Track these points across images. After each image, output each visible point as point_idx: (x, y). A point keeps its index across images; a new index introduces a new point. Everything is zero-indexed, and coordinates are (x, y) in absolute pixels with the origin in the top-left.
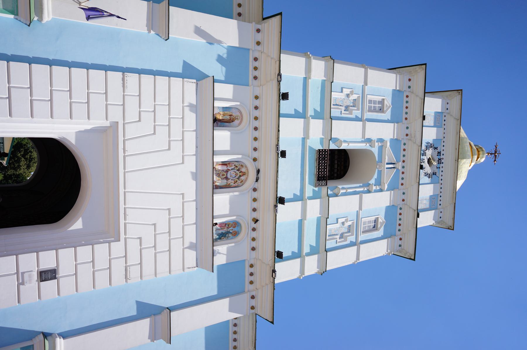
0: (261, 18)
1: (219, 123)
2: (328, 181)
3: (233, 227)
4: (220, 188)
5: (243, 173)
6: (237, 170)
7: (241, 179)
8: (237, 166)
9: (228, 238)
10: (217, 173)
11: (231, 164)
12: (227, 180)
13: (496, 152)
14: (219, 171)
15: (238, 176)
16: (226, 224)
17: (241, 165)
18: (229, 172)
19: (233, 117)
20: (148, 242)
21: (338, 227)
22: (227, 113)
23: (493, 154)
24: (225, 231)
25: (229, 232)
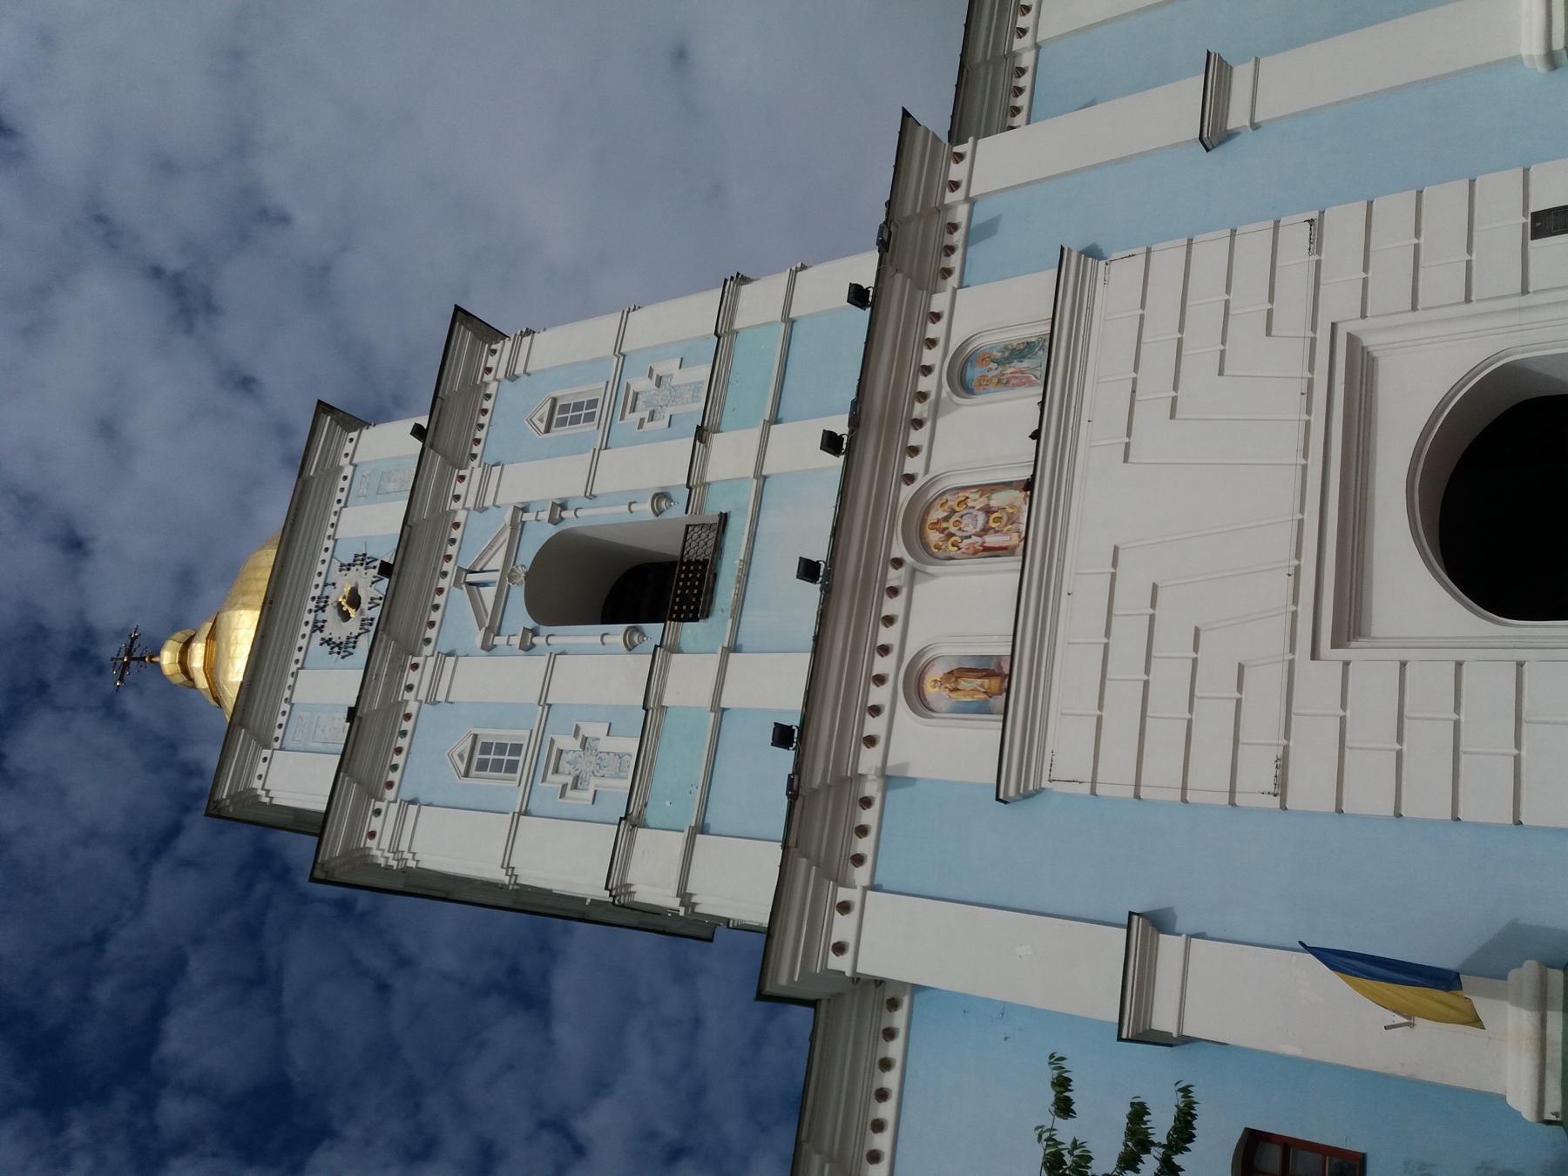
0: (823, 1008)
1: (992, 668)
3: (987, 376)
4: (1012, 482)
5: (938, 527)
6: (952, 535)
7: (944, 511)
8: (953, 545)
9: (1006, 348)
10: (1014, 526)
11: (971, 550)
12: (988, 505)
13: (126, 665)
14: (1008, 530)
15: (954, 519)
17: (939, 550)
18: (978, 530)
19: (948, 686)
21: (671, 406)
22: (965, 696)
23: (135, 659)
24: (1013, 365)
25: (998, 363)
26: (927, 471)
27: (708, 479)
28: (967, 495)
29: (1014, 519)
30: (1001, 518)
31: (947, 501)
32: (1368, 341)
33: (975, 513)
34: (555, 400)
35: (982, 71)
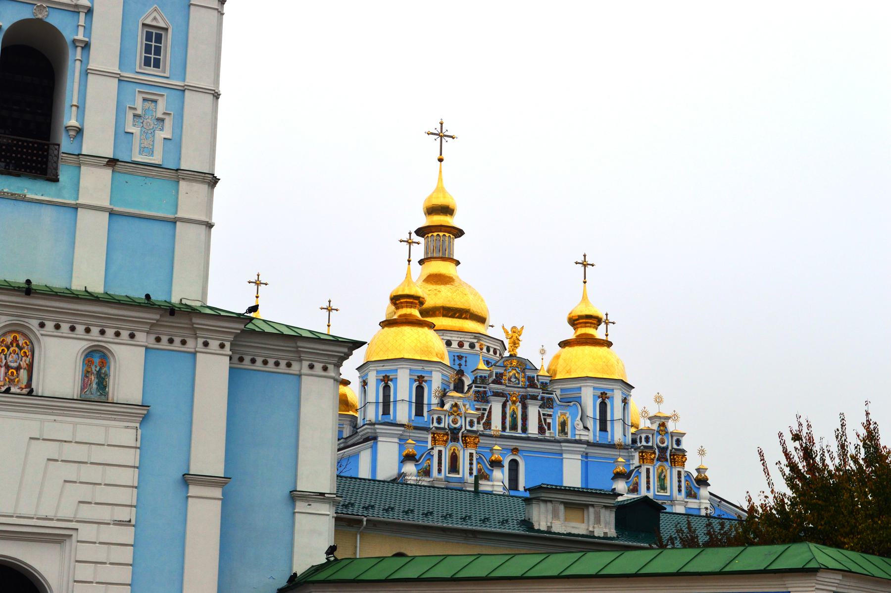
2: (52, 141)
4: (31, 381)
5: (14, 341)
6: (8, 348)
7: (22, 344)
8: (3, 350)
9: (107, 375)
10: (7, 383)
12: (21, 368)
14: (6, 380)
15: (17, 350)
16: (87, 377)
18: (9, 363)
20: (85, 493)
21: (141, 130)
26: (42, 335)
27: (83, 168)
28: (29, 357)
29: (11, 383)
30: (13, 376)
31: (28, 345)
32: (68, 543)
33: (18, 362)
34: (166, 30)
35: (294, 345)
